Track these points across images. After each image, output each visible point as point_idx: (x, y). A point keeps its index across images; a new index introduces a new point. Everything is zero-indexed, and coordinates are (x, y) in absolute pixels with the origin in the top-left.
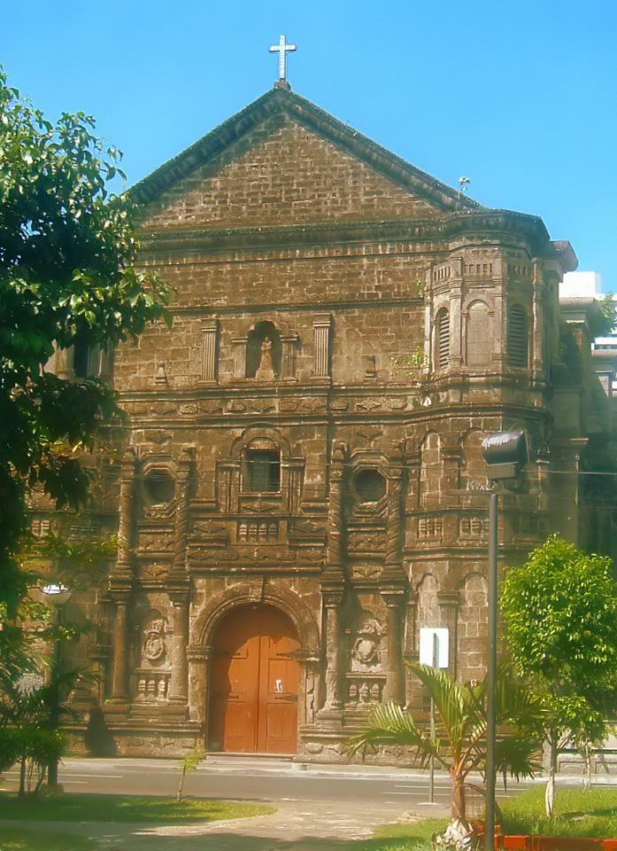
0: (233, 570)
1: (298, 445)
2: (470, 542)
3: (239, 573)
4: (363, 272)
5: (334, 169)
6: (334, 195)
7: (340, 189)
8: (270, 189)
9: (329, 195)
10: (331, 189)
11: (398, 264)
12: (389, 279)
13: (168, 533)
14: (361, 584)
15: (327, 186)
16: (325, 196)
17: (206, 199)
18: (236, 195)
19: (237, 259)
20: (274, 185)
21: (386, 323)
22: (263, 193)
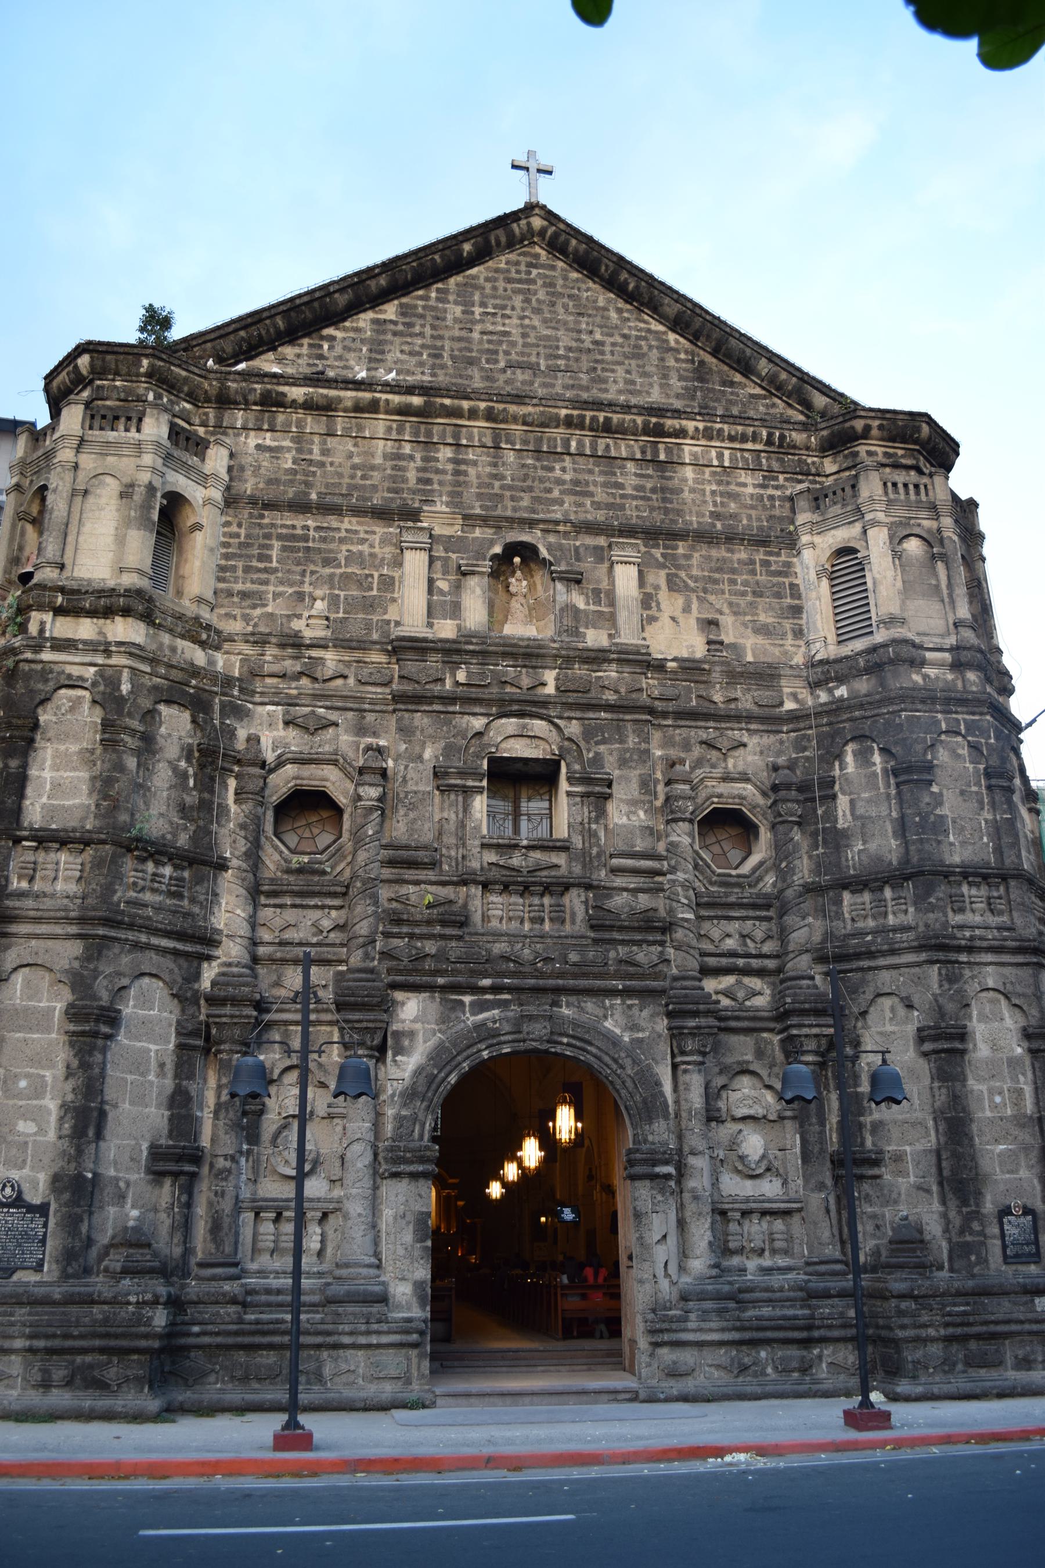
0: (486, 982)
1: (597, 754)
2: (977, 932)
3: (495, 989)
4: (686, 489)
5: (625, 336)
6: (628, 372)
7: (638, 366)
8: (519, 348)
9: (620, 371)
10: (623, 363)
11: (745, 485)
12: (733, 505)
13: (330, 907)
14: (737, 1018)
15: (616, 358)
16: (613, 371)
17: (406, 348)
18: (460, 350)
19: (464, 442)
20: (525, 345)
21: (733, 571)
22: (507, 353)
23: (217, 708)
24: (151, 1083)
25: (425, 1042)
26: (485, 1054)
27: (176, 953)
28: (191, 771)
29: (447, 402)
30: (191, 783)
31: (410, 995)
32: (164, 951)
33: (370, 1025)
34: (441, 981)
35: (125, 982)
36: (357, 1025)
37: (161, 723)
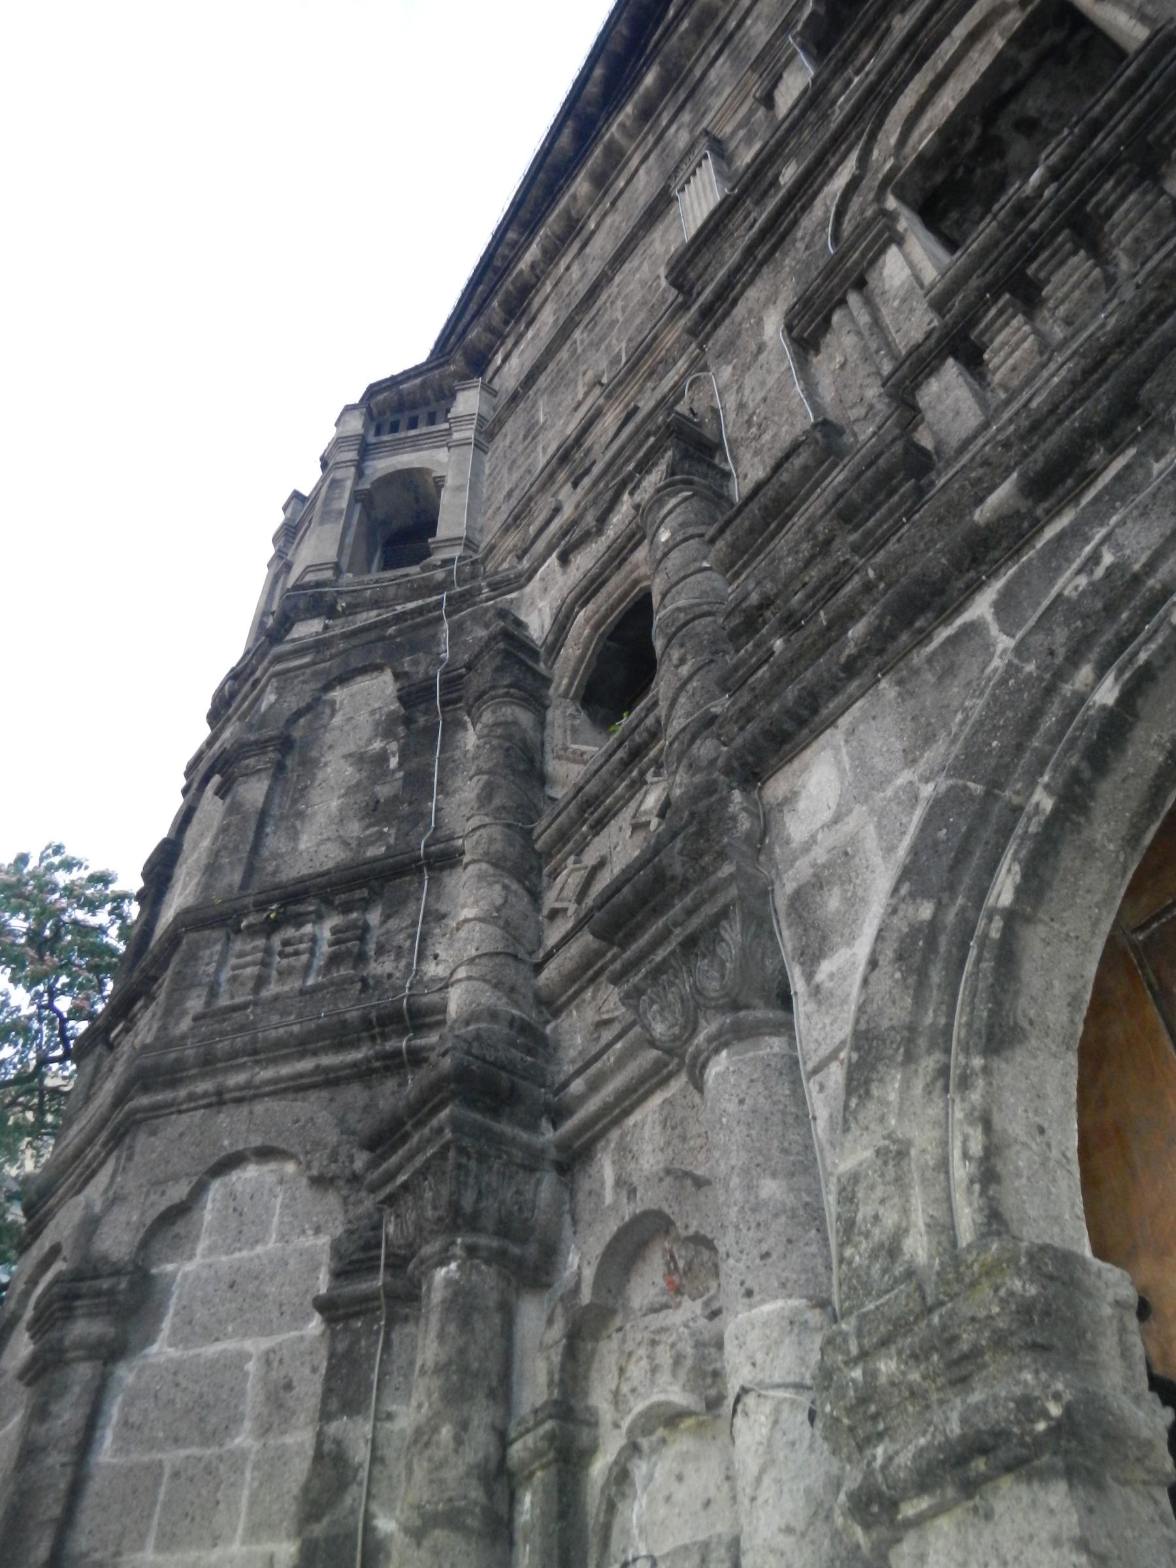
0: (1003, 494)
23: (446, 635)
24: (237, 1461)
25: (890, 849)
26: (1107, 694)
27: (331, 1080)
28: (393, 746)
29: (685, 24)
30: (394, 762)
31: (807, 754)
32: (297, 1087)
33: (695, 922)
34: (857, 631)
35: (178, 1192)
36: (660, 955)
37: (333, 713)
